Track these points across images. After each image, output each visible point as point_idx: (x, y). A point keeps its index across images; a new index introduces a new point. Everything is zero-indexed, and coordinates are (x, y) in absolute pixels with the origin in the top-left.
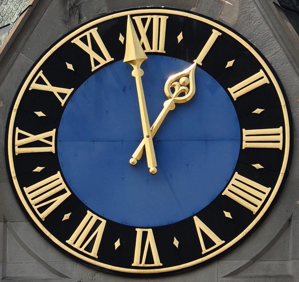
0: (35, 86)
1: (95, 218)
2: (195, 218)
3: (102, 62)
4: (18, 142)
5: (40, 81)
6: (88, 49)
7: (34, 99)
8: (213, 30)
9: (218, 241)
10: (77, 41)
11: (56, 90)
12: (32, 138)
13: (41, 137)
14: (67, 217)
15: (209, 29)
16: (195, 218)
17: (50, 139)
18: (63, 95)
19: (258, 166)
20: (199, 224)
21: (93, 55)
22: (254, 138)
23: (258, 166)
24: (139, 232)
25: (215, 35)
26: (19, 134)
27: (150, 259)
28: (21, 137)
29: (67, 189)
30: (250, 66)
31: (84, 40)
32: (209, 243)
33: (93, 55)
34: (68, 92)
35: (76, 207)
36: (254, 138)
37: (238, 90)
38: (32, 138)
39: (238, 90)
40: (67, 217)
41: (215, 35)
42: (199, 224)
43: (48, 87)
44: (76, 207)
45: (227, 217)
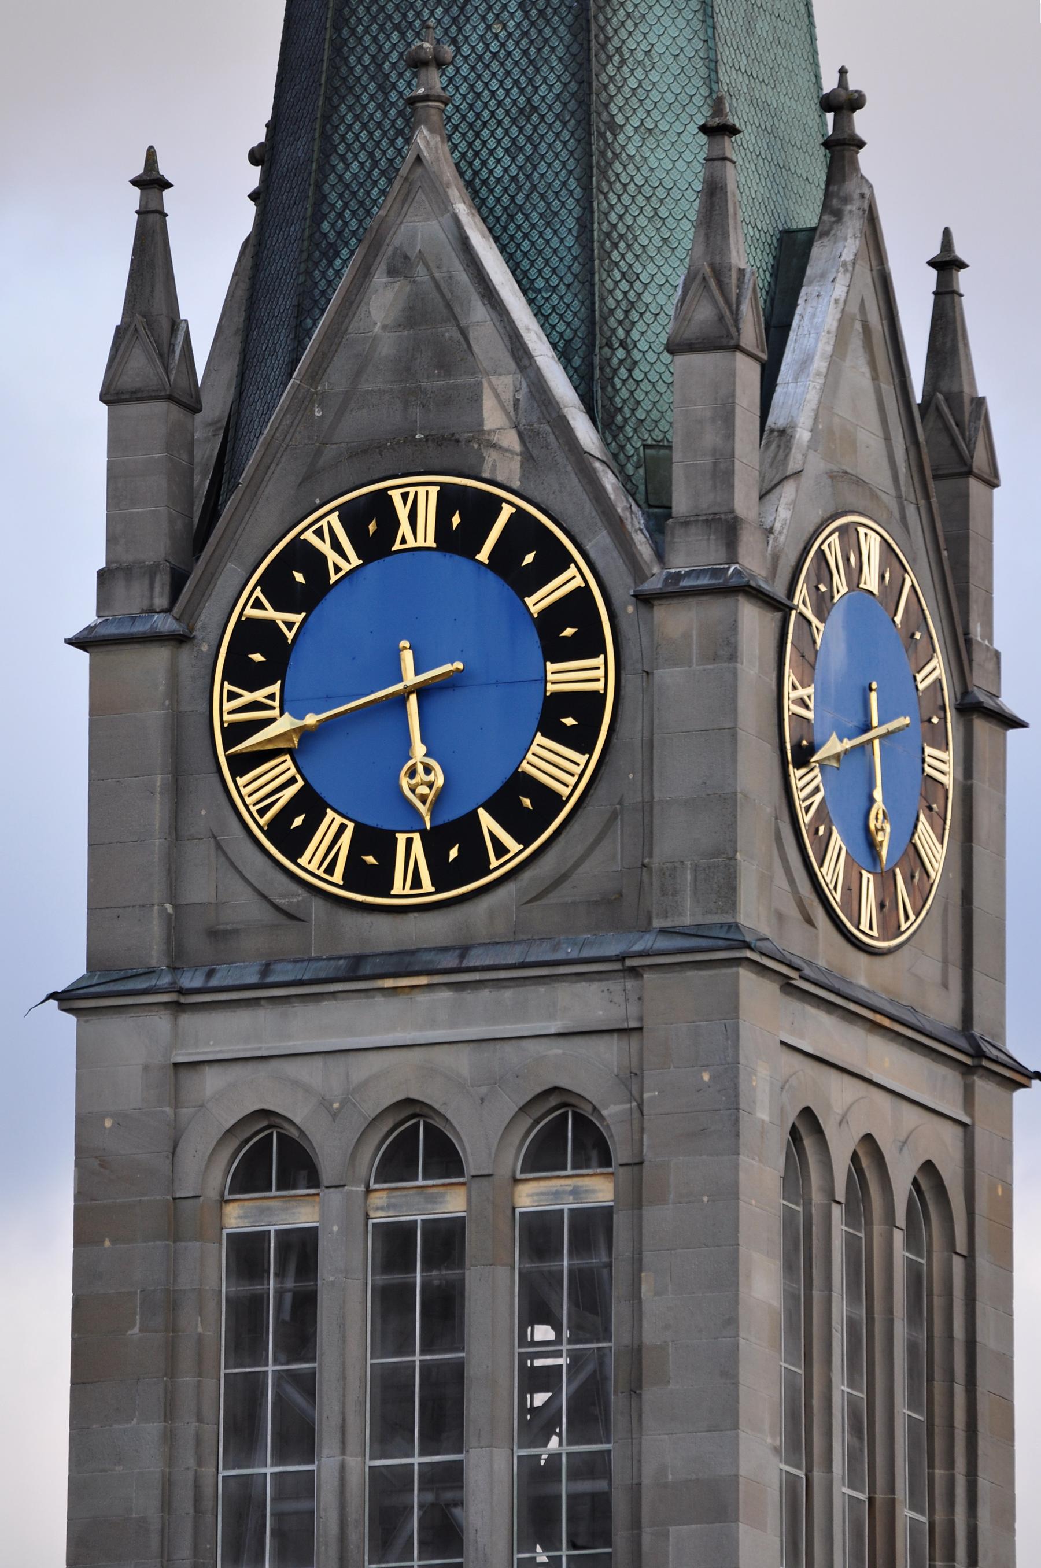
0: (250, 612)
1: (339, 820)
2: (481, 811)
3: (346, 567)
4: (227, 706)
5: (258, 605)
6: (325, 547)
7: (254, 634)
8: (504, 505)
9: (512, 845)
10: (309, 536)
11: (280, 617)
12: (248, 697)
13: (259, 695)
14: (298, 821)
15: (497, 503)
16: (481, 811)
17: (271, 697)
18: (290, 625)
19: (569, 721)
20: (487, 821)
21: (332, 557)
22: (565, 676)
23: (569, 721)
24: (401, 838)
25: (507, 511)
26: (229, 691)
27: (417, 883)
28: (232, 696)
29: (298, 777)
30: (555, 561)
31: (319, 532)
32: (501, 850)
33: (332, 557)
34: (297, 618)
35: (311, 804)
36: (565, 676)
37: (537, 602)
38: (248, 697)
39: (537, 602)
40: (298, 821)
41: (507, 511)
42: (487, 821)
43: (270, 613)
44: (311, 804)
45: (525, 805)
